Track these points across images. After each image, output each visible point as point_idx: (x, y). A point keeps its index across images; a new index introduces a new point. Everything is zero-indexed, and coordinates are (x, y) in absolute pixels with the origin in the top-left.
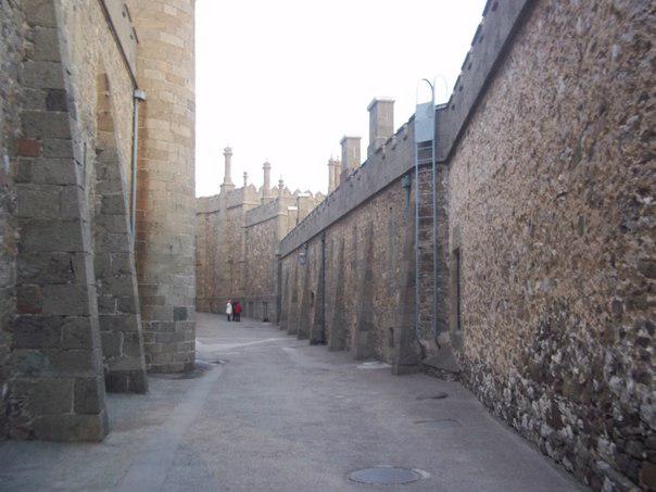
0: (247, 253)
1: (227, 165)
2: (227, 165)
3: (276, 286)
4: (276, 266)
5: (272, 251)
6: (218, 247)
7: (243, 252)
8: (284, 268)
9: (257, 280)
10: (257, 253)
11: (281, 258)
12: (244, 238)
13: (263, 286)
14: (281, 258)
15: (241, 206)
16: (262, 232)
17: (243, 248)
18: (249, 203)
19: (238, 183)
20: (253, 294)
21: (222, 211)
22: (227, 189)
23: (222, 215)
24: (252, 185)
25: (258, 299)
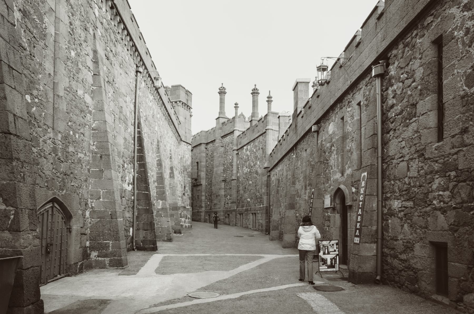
0: (238, 172)
1: (222, 102)
2: (222, 102)
3: (265, 198)
4: (265, 178)
5: (260, 166)
6: (215, 169)
7: (235, 172)
8: (273, 178)
9: (246, 195)
10: (246, 170)
11: (270, 170)
12: (235, 160)
13: (251, 199)
14: (270, 170)
15: (232, 132)
16: (251, 151)
17: (235, 168)
18: (240, 127)
19: (230, 113)
20: (243, 207)
21: (217, 141)
22: (222, 120)
23: (217, 144)
24: (242, 115)
25: (247, 210)
